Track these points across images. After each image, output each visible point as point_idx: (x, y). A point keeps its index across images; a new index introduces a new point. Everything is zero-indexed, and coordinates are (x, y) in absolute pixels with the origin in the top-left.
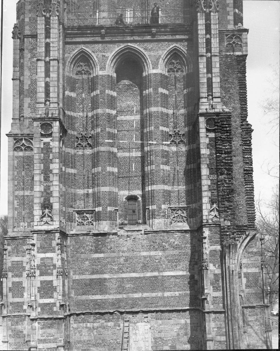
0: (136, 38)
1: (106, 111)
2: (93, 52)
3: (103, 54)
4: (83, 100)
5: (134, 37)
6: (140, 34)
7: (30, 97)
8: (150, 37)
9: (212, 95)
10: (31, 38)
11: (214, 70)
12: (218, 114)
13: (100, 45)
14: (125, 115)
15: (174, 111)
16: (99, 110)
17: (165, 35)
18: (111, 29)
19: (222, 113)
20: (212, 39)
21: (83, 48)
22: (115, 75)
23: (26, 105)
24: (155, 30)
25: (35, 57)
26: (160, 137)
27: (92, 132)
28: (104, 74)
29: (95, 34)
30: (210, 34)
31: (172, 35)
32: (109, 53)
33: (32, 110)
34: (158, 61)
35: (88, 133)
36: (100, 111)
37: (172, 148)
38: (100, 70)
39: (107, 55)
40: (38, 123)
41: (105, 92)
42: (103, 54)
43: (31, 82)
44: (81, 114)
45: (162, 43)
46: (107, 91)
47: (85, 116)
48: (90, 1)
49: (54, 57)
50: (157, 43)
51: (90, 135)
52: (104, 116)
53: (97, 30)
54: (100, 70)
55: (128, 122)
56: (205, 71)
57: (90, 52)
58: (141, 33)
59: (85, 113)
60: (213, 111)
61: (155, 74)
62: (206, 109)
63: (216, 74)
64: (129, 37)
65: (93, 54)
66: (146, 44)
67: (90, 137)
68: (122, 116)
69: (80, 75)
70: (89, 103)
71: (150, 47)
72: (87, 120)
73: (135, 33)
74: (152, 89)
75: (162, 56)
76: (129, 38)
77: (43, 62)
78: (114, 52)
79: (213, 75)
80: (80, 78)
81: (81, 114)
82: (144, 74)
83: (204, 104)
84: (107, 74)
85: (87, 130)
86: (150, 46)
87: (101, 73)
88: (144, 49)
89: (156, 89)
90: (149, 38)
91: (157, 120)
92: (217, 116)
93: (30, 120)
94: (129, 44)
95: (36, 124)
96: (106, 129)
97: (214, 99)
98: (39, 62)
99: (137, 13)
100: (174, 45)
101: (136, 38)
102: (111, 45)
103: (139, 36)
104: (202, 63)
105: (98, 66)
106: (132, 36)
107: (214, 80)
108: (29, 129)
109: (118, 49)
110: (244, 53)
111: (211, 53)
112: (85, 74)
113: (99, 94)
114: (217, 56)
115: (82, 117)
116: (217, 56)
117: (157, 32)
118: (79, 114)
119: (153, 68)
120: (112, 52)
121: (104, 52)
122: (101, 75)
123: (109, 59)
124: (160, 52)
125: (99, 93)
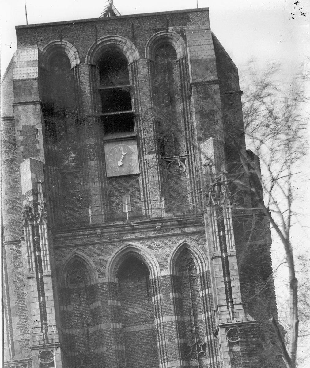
0: (139, 236)
1: (110, 327)
2: (88, 256)
3: (101, 257)
4: (82, 313)
5: (136, 234)
6: (142, 231)
7: (19, 316)
8: (155, 232)
9: (232, 302)
10: (13, 244)
11: (232, 273)
12: (239, 325)
13: (97, 246)
14: (132, 326)
15: (190, 317)
16: (102, 325)
17: (172, 229)
18: (108, 228)
19: (247, 323)
20: (227, 236)
21: (77, 252)
22: (117, 281)
23: (15, 326)
24: (160, 224)
25: (19, 267)
26: (176, 352)
27: (96, 351)
28: (104, 281)
29: (89, 234)
30: (224, 231)
31: (180, 228)
32: (107, 256)
33: (23, 331)
34: (166, 260)
35: (92, 352)
36: (103, 326)
37: (192, 362)
38: (99, 277)
39: (105, 259)
40: (37, 351)
41: (107, 303)
42: (101, 257)
43: (18, 297)
44: (80, 331)
45: (170, 238)
46: (109, 301)
47: (86, 332)
48: (78, 190)
49: (47, 273)
50: (163, 239)
51: (94, 355)
52: (109, 332)
53: (92, 230)
54: (99, 277)
55: (136, 333)
56: (222, 274)
57: (85, 256)
58: (144, 229)
59: (86, 329)
60: (234, 321)
61: (164, 276)
62: (228, 319)
63: (234, 277)
64: (129, 235)
65: (89, 259)
66: (150, 242)
67: (94, 357)
68: (129, 326)
69: (76, 284)
70: (89, 317)
71: (156, 245)
72: (88, 337)
73: (136, 229)
74: (161, 295)
75: (171, 255)
76: (130, 236)
77: (35, 280)
78: (114, 254)
79: (232, 278)
80: (76, 287)
81: (80, 331)
82: (152, 277)
83: (224, 313)
84: (107, 281)
85: (89, 349)
86: (156, 243)
87: (100, 281)
88: (149, 247)
89: (166, 295)
90: (153, 233)
91: (171, 331)
92: (239, 326)
93: (21, 343)
94: (130, 243)
95: (34, 353)
96: (112, 347)
97: (235, 306)
98: (31, 280)
99: (135, 200)
100: (183, 240)
101: (139, 236)
102: (110, 246)
103: (141, 232)
104: (218, 266)
105: (96, 273)
106: (133, 233)
107: (233, 284)
108: (21, 354)
109: (118, 249)
110: (268, 242)
111: (226, 251)
112: (81, 282)
113: (101, 307)
114: (233, 256)
115: (81, 335)
116: (233, 256)
117: (162, 227)
118: (78, 330)
119: (161, 270)
120: (110, 255)
121: (102, 255)
122: (100, 283)
123: (108, 263)
124: (168, 250)
125: (100, 305)
